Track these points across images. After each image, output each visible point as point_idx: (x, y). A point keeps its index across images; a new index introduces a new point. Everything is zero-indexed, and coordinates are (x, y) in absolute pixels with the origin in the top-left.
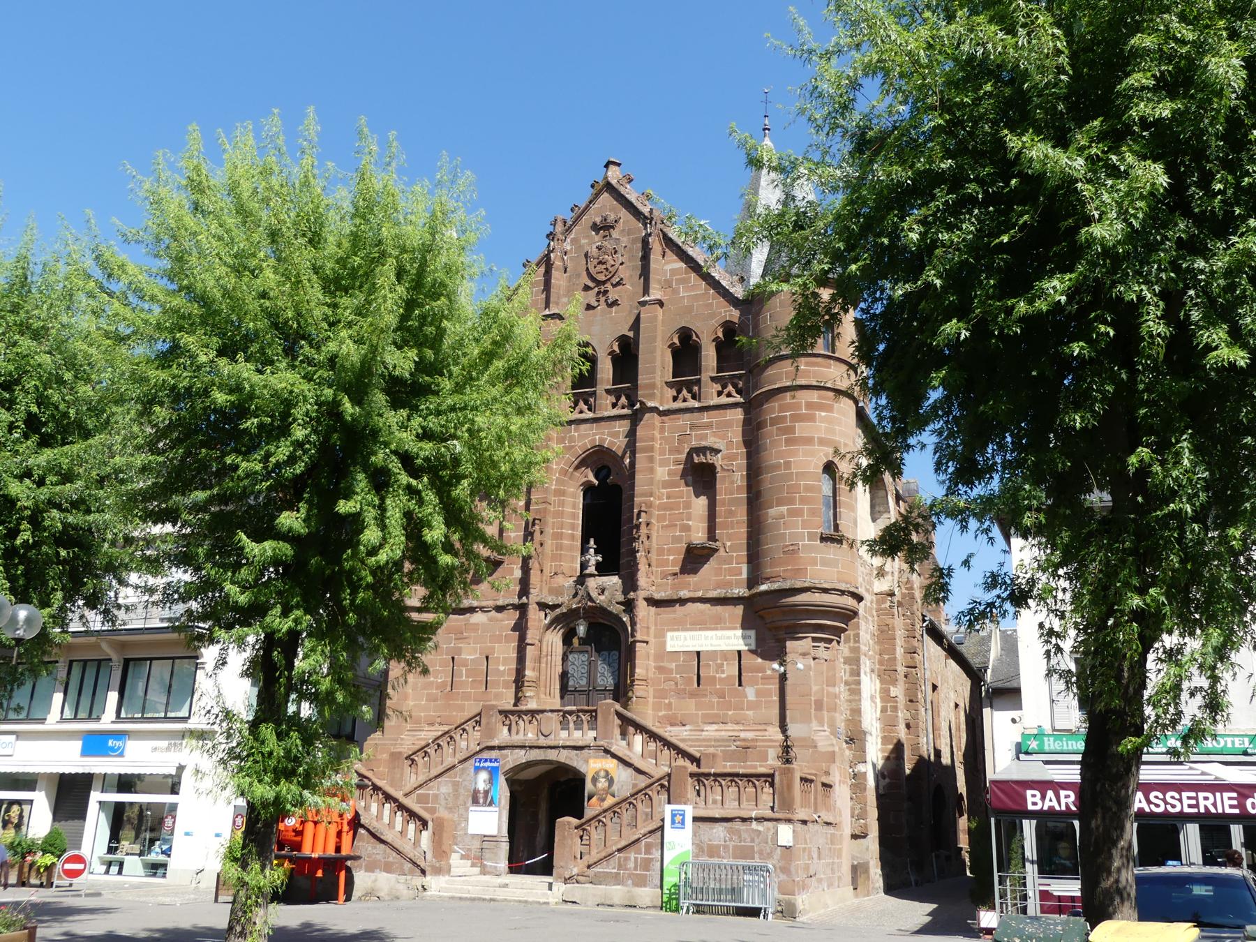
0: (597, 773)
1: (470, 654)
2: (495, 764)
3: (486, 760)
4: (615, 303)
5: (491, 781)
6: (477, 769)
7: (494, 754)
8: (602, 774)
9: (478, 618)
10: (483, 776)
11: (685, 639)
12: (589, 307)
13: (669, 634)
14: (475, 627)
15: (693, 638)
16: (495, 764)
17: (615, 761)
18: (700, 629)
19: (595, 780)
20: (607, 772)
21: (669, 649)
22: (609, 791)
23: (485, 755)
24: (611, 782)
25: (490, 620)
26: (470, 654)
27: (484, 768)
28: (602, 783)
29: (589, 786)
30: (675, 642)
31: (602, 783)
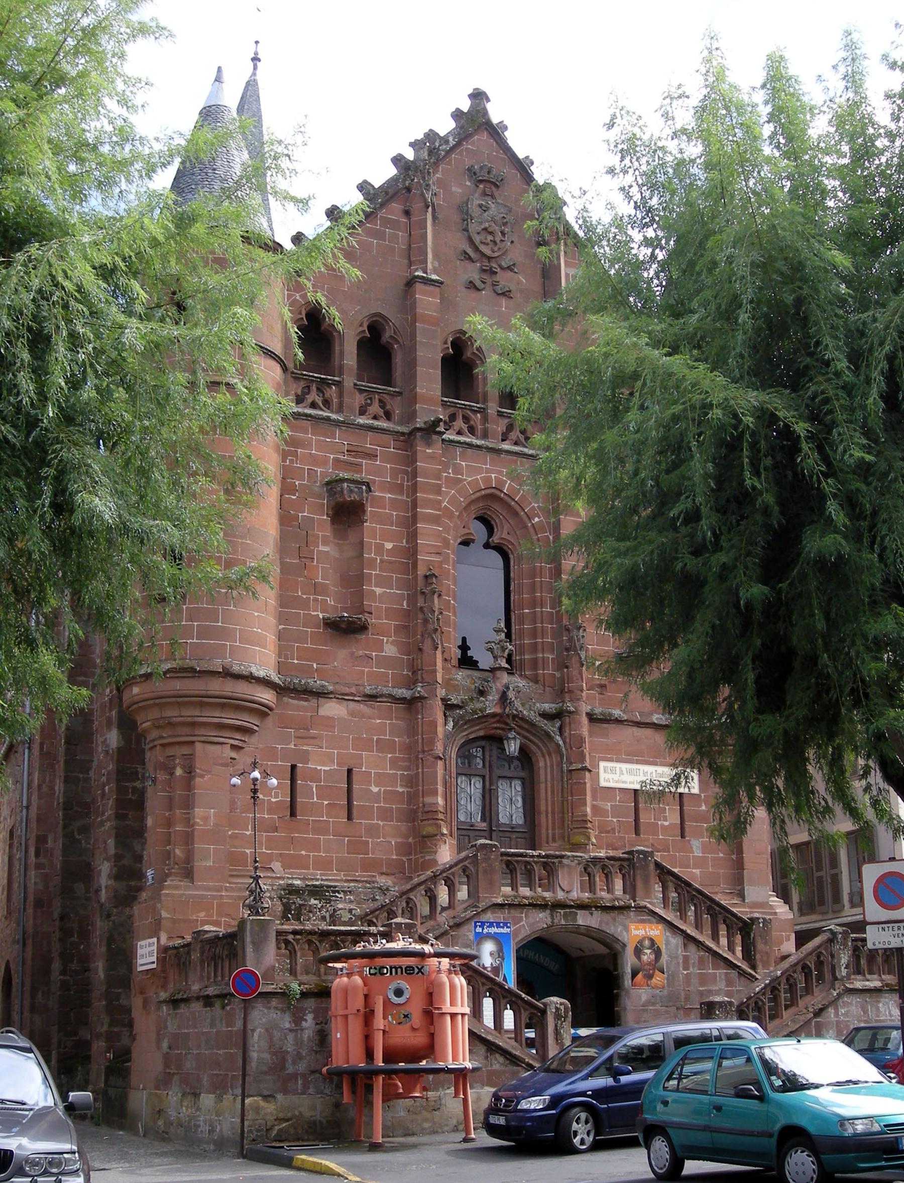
0: (641, 942)
1: (323, 764)
2: (505, 930)
3: (491, 925)
4: (506, 294)
5: (500, 953)
6: (481, 938)
7: (500, 916)
8: (647, 943)
9: (332, 709)
10: (488, 947)
11: (622, 773)
12: (471, 286)
13: (602, 764)
14: (329, 722)
15: (630, 772)
16: (505, 930)
17: (660, 926)
18: (638, 762)
19: (638, 952)
20: (652, 941)
21: (603, 783)
22: (656, 966)
23: (489, 917)
24: (658, 953)
25: (352, 714)
26: (323, 764)
27: (489, 936)
28: (648, 956)
29: (629, 961)
30: (610, 776)
31: (648, 956)
